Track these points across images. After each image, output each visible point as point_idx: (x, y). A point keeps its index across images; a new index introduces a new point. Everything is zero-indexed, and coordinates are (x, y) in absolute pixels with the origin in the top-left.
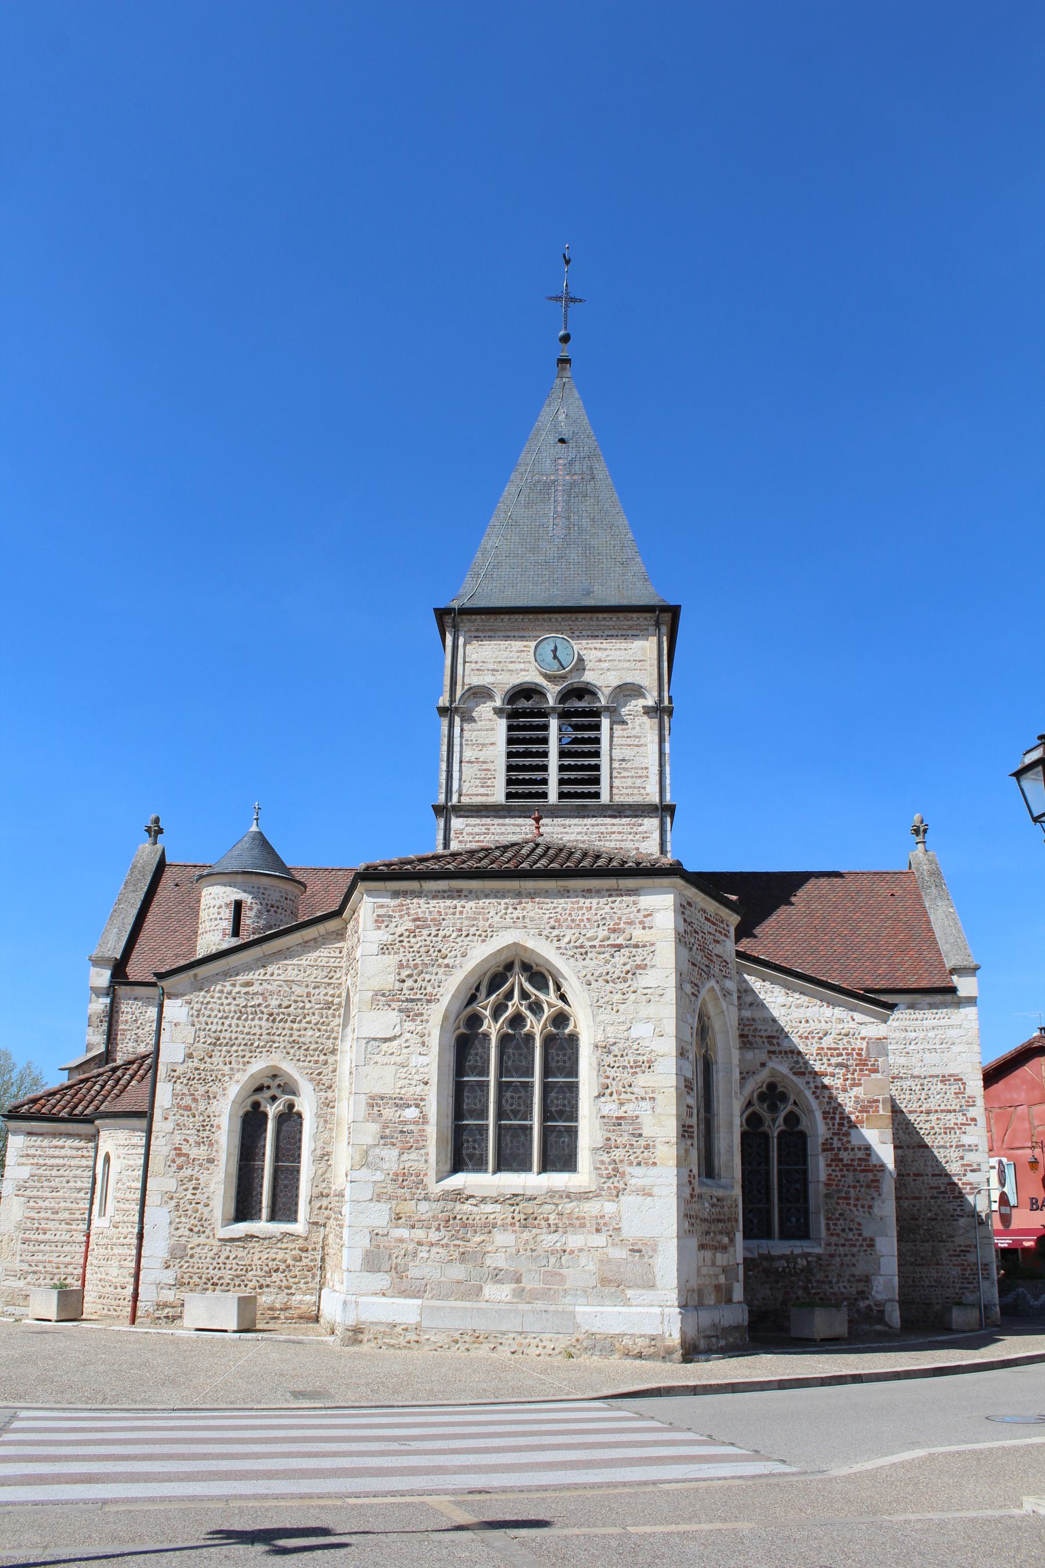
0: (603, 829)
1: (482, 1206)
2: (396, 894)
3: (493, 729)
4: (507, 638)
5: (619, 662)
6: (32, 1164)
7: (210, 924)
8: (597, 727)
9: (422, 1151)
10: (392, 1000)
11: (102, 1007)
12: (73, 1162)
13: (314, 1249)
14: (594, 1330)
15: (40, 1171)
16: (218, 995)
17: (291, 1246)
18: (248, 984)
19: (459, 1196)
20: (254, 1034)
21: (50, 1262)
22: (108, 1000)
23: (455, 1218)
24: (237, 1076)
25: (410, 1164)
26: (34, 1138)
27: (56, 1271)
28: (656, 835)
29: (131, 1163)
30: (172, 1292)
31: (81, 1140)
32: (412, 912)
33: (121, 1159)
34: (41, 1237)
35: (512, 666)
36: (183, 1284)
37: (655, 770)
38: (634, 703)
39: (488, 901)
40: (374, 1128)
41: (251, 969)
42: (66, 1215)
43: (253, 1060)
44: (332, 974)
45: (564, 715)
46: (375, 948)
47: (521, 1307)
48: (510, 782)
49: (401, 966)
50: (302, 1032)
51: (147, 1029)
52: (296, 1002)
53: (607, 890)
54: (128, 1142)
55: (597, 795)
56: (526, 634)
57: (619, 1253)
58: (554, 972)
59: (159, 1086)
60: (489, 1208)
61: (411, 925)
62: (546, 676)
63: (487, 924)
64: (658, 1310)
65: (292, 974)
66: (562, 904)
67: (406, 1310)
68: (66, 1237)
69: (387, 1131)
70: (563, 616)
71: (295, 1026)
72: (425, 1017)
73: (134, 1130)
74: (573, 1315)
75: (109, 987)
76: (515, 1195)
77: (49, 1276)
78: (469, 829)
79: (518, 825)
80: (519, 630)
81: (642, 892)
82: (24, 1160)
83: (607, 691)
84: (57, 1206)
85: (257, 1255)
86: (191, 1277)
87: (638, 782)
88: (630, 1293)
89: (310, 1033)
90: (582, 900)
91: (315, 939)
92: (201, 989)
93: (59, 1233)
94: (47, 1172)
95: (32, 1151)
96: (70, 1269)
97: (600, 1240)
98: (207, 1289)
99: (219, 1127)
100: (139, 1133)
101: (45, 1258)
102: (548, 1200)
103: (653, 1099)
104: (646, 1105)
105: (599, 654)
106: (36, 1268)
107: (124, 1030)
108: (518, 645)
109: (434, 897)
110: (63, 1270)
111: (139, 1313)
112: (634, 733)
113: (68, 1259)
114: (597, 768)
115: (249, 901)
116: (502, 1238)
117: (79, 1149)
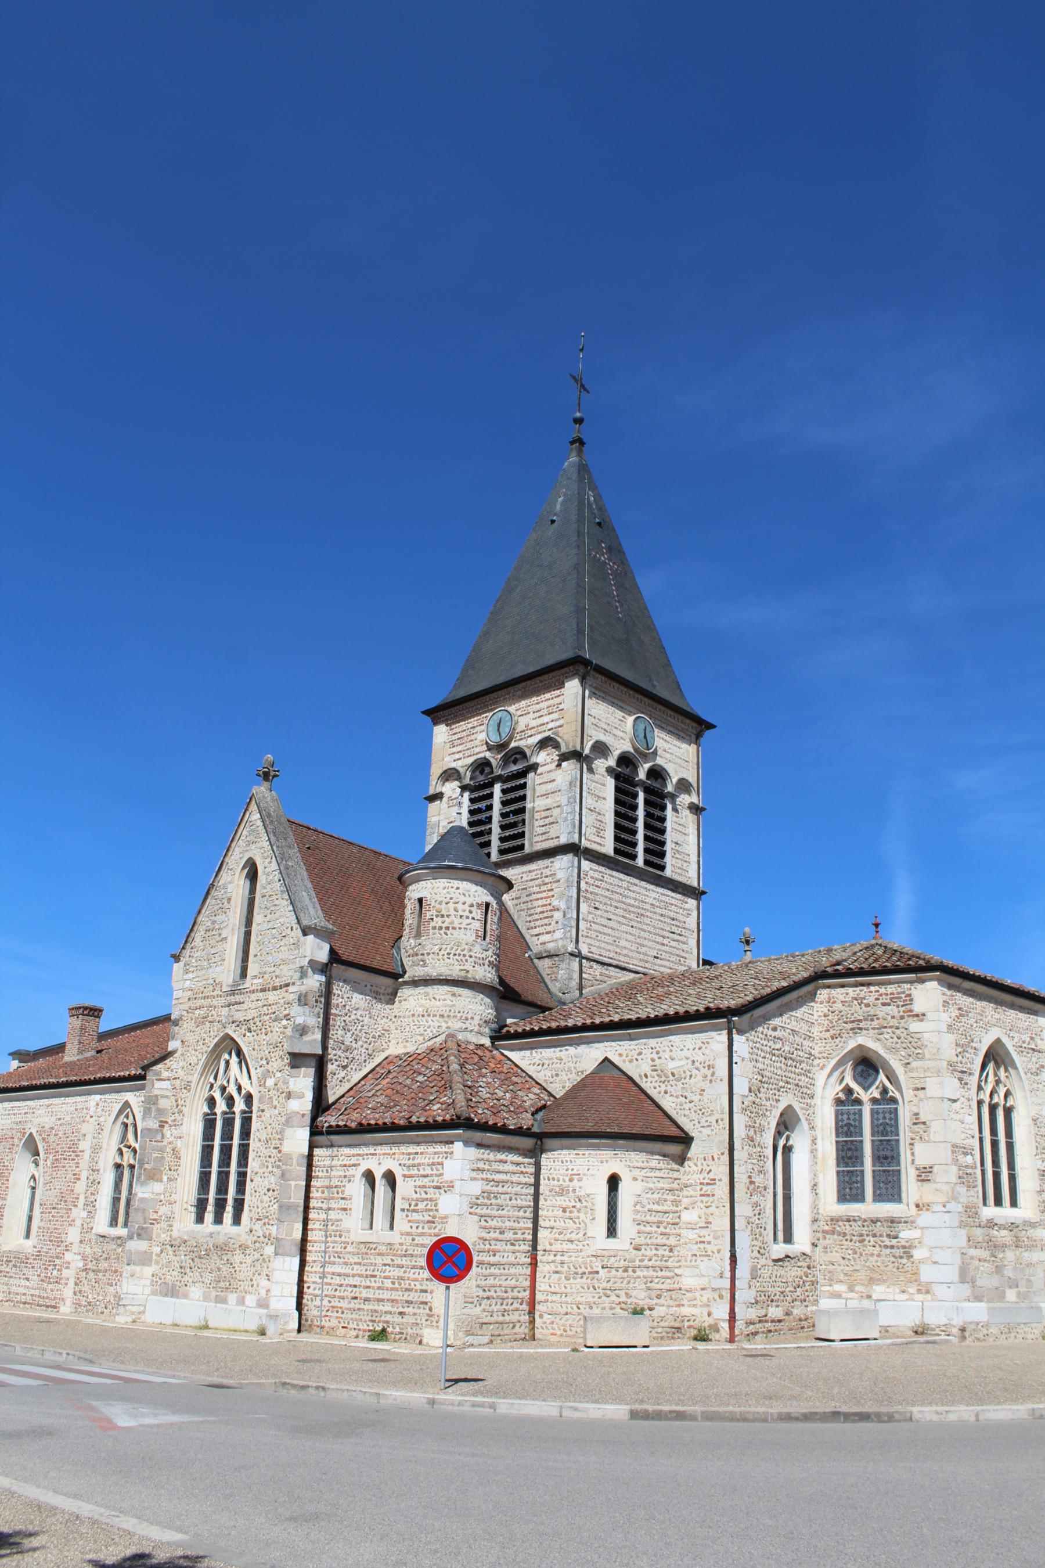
0: (667, 899)
2: (950, 987)
3: (604, 785)
4: (613, 704)
5: (677, 757)
6: (483, 1179)
7: (460, 920)
8: (663, 808)
11: (318, 984)
12: (515, 1178)
15: (488, 1188)
18: (775, 1029)
19: (991, 1224)
21: (500, 1286)
22: (323, 979)
24: (774, 1110)
25: (971, 1199)
26: (482, 1151)
27: (505, 1295)
28: (695, 914)
29: (651, 1185)
30: (754, 1310)
31: (520, 1155)
33: (639, 1183)
34: (492, 1260)
35: (615, 732)
36: (757, 1302)
37: (694, 858)
38: (682, 796)
40: (954, 1169)
41: (775, 1016)
42: (509, 1235)
45: (647, 790)
46: (944, 1028)
48: (617, 839)
49: (957, 1045)
51: (353, 1017)
54: (645, 1164)
55: (662, 868)
56: (624, 706)
58: (1007, 1061)
59: (735, 1116)
60: (1004, 1233)
61: (957, 1013)
62: (636, 750)
66: (1012, 1014)
67: (977, 1312)
68: (512, 1259)
70: (650, 701)
73: (652, 1153)
75: (327, 964)
77: (499, 1302)
78: (591, 873)
79: (621, 880)
80: (620, 700)
82: (474, 1174)
83: (674, 780)
84: (503, 1225)
85: (791, 1272)
87: (685, 864)
89: (803, 1078)
92: (752, 1029)
93: (506, 1255)
94: (494, 1188)
95: (481, 1165)
96: (515, 1294)
100: (657, 1157)
101: (497, 1282)
105: (666, 746)
106: (488, 1294)
107: (336, 1015)
108: (619, 714)
109: (965, 994)
110: (510, 1294)
111: (737, 1332)
112: (682, 822)
113: (513, 1282)
114: (663, 844)
115: (495, 906)
116: (1010, 1255)
117: (518, 1164)
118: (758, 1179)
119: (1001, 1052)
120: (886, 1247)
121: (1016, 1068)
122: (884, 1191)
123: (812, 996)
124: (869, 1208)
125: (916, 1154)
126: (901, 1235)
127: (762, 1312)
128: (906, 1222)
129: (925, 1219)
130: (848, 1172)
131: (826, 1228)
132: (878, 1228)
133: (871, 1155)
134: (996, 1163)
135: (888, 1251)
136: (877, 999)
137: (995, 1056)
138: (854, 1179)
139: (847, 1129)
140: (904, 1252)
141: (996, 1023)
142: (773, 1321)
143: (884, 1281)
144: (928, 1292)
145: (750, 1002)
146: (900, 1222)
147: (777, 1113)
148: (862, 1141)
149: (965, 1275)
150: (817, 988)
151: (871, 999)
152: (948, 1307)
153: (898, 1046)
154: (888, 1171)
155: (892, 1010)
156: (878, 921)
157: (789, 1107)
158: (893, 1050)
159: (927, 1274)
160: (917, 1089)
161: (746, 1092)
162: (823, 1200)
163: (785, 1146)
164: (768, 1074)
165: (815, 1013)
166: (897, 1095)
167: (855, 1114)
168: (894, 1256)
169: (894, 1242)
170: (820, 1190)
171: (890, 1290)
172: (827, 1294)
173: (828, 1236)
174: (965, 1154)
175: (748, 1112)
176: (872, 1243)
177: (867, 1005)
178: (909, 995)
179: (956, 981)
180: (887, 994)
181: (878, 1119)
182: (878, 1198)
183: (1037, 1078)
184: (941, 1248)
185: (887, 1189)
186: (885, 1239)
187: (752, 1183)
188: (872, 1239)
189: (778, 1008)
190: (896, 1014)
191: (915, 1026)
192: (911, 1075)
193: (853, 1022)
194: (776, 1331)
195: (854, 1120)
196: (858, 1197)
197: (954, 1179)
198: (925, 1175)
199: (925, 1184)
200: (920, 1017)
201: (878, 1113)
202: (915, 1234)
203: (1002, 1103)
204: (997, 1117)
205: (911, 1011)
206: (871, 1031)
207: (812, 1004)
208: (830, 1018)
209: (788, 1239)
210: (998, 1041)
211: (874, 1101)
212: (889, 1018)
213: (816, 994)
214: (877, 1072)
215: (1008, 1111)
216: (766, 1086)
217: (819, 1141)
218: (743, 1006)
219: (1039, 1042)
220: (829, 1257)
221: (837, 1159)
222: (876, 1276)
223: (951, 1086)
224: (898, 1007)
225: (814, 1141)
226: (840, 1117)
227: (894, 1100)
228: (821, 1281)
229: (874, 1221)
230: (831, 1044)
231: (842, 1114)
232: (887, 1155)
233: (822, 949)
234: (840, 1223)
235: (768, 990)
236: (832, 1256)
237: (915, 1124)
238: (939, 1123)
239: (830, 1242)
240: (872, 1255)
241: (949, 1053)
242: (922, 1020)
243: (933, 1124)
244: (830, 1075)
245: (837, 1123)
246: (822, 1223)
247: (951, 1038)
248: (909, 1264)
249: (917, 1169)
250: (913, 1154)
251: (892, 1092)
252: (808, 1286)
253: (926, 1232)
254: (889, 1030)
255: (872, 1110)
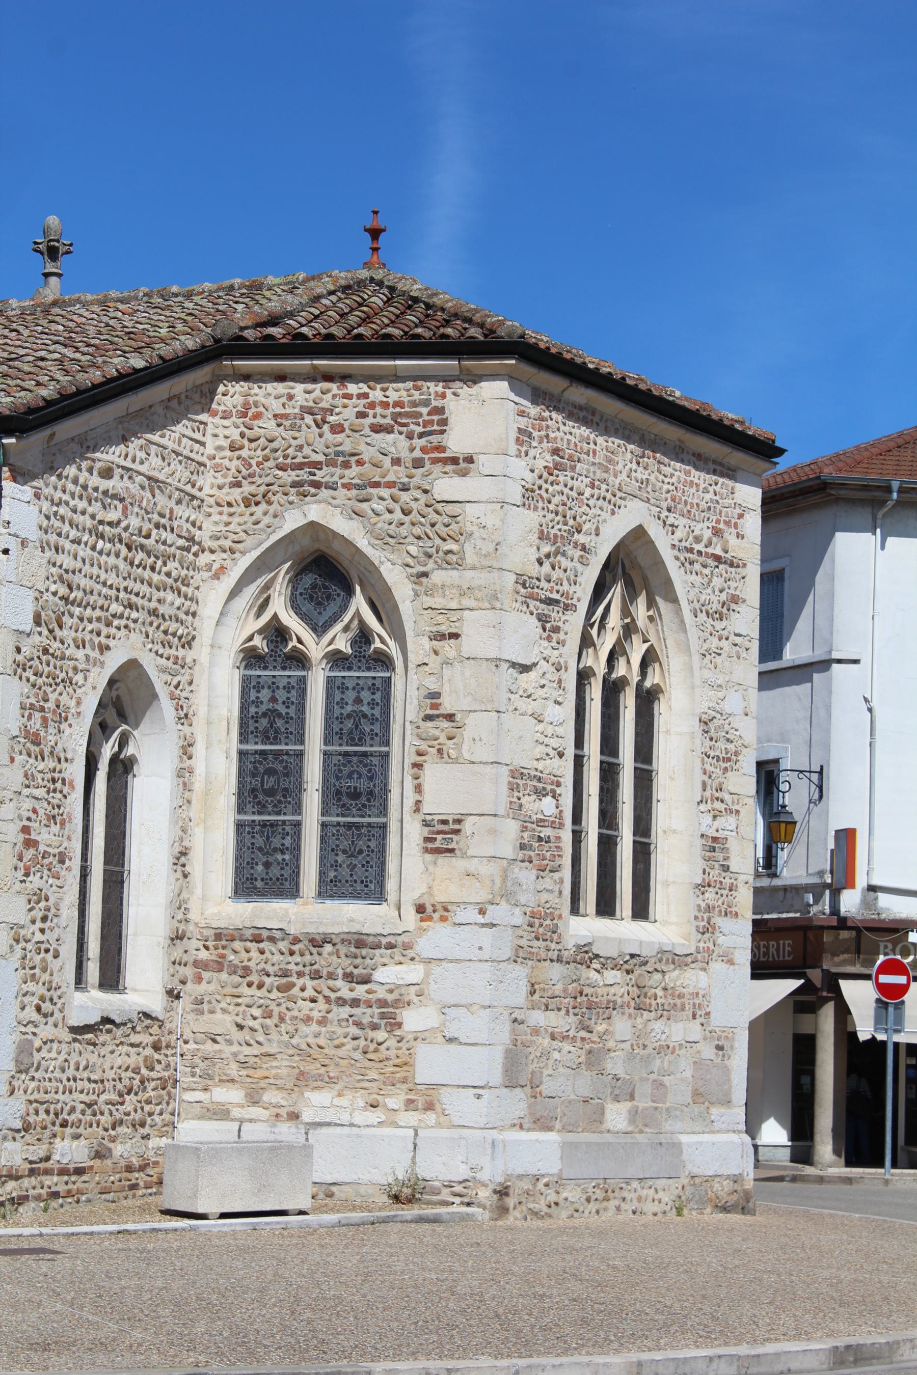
1: (606, 972)
2: (538, 396)
9: (556, 876)
10: (531, 597)
13: (168, 1046)
14: (696, 1171)
16: (70, 486)
17: (146, 1039)
18: (107, 473)
19: (586, 956)
20: (111, 587)
23: (581, 993)
25: (545, 896)
30: (18, 1145)
32: (552, 435)
36: (27, 1128)
39: (617, 441)
40: (511, 828)
43: (112, 643)
44: (195, 477)
47: (640, 1138)
50: (162, 594)
52: (157, 526)
53: (714, 462)
57: (708, 1052)
58: (654, 582)
60: (612, 976)
63: (617, 482)
64: (735, 1137)
65: (153, 465)
66: (677, 471)
67: (539, 1153)
69: (526, 835)
71: (156, 578)
72: (561, 636)
74: (677, 1147)
76: (632, 956)
81: (739, 474)
86: (37, 1113)
88: (715, 1111)
89: (170, 596)
90: (693, 471)
91: (177, 397)
92: (51, 469)
97: (694, 1030)
98: (55, 1136)
99: (72, 787)
102: (658, 966)
103: (738, 812)
104: (729, 822)
109: (570, 416)
116: (622, 1026)
118: (45, 837)
119: (644, 560)
120: (341, 1002)
121: (675, 600)
122: (345, 872)
123: (204, 398)
124: (305, 911)
125: (426, 788)
126: (378, 976)
127: (41, 1151)
128: (391, 946)
129: (436, 939)
130: (264, 824)
131: (203, 955)
132: (327, 958)
133: (321, 786)
134: (608, 817)
135: (345, 1012)
136: (362, 415)
137: (630, 569)
138: (276, 842)
139: (267, 723)
140: (383, 1016)
141: (641, 493)
142: (63, 1172)
143: (332, 1081)
144: (429, 1107)
145: (49, 403)
146: (378, 946)
147: (100, 678)
148: (300, 755)
149: (517, 1071)
150: (218, 379)
151: (347, 415)
152: (475, 1139)
153: (403, 531)
154: (358, 826)
155: (396, 443)
156: (381, 222)
157: (132, 665)
158: (387, 540)
159: (431, 1064)
160: (441, 637)
161: (27, 624)
162: (198, 891)
163: (114, 760)
164: (85, 582)
165: (208, 440)
166: (393, 648)
167: (288, 688)
168: (358, 1024)
169: (360, 990)
170: (195, 866)
171: (344, 1101)
172: (197, 1108)
173: (206, 975)
174: (540, 793)
175: (29, 673)
176: (309, 993)
177: (337, 429)
178: (440, 411)
179: (554, 383)
180: (385, 405)
181: (342, 703)
182: (330, 888)
183: (719, 625)
184: (468, 1007)
185: (352, 867)
186: (340, 983)
187: (30, 843)
188: (310, 984)
189: (120, 420)
190: (405, 455)
191: (446, 486)
192: (428, 601)
193: (300, 466)
194: (69, 1194)
195: (287, 703)
196: (287, 887)
197: (508, 850)
198: (443, 837)
199: (442, 860)
200: (462, 464)
201: (343, 688)
202: (411, 973)
203: (635, 678)
204: (619, 711)
205: (440, 448)
206: (342, 492)
207: (203, 417)
208: (245, 453)
209: (112, 978)
210: (639, 533)
211: (336, 659)
212: (387, 461)
213: (213, 393)
214: (350, 592)
215: (647, 699)
216: (77, 611)
217: (199, 750)
218: (31, 411)
219: (733, 541)
220: (206, 1023)
221: (240, 794)
222: (312, 1068)
223: (520, 634)
224: (410, 437)
225: (187, 750)
226: (253, 695)
227: (383, 660)
228: (185, 1080)
229: (317, 943)
230: (241, 518)
231: (258, 688)
232: (359, 789)
233: (237, 281)
234: (237, 945)
235: (96, 376)
236: (214, 1020)
237: (428, 718)
238: (484, 712)
239: (212, 988)
240: (308, 1020)
241: (522, 555)
242: (464, 474)
243: (471, 720)
244: (234, 593)
245: (244, 708)
246: (195, 944)
247: (531, 519)
248: (392, 1043)
249: (426, 824)
250: (418, 789)
251: (382, 639)
252: (152, 1091)
253: (436, 970)
254: (385, 493)
255: (330, 681)
